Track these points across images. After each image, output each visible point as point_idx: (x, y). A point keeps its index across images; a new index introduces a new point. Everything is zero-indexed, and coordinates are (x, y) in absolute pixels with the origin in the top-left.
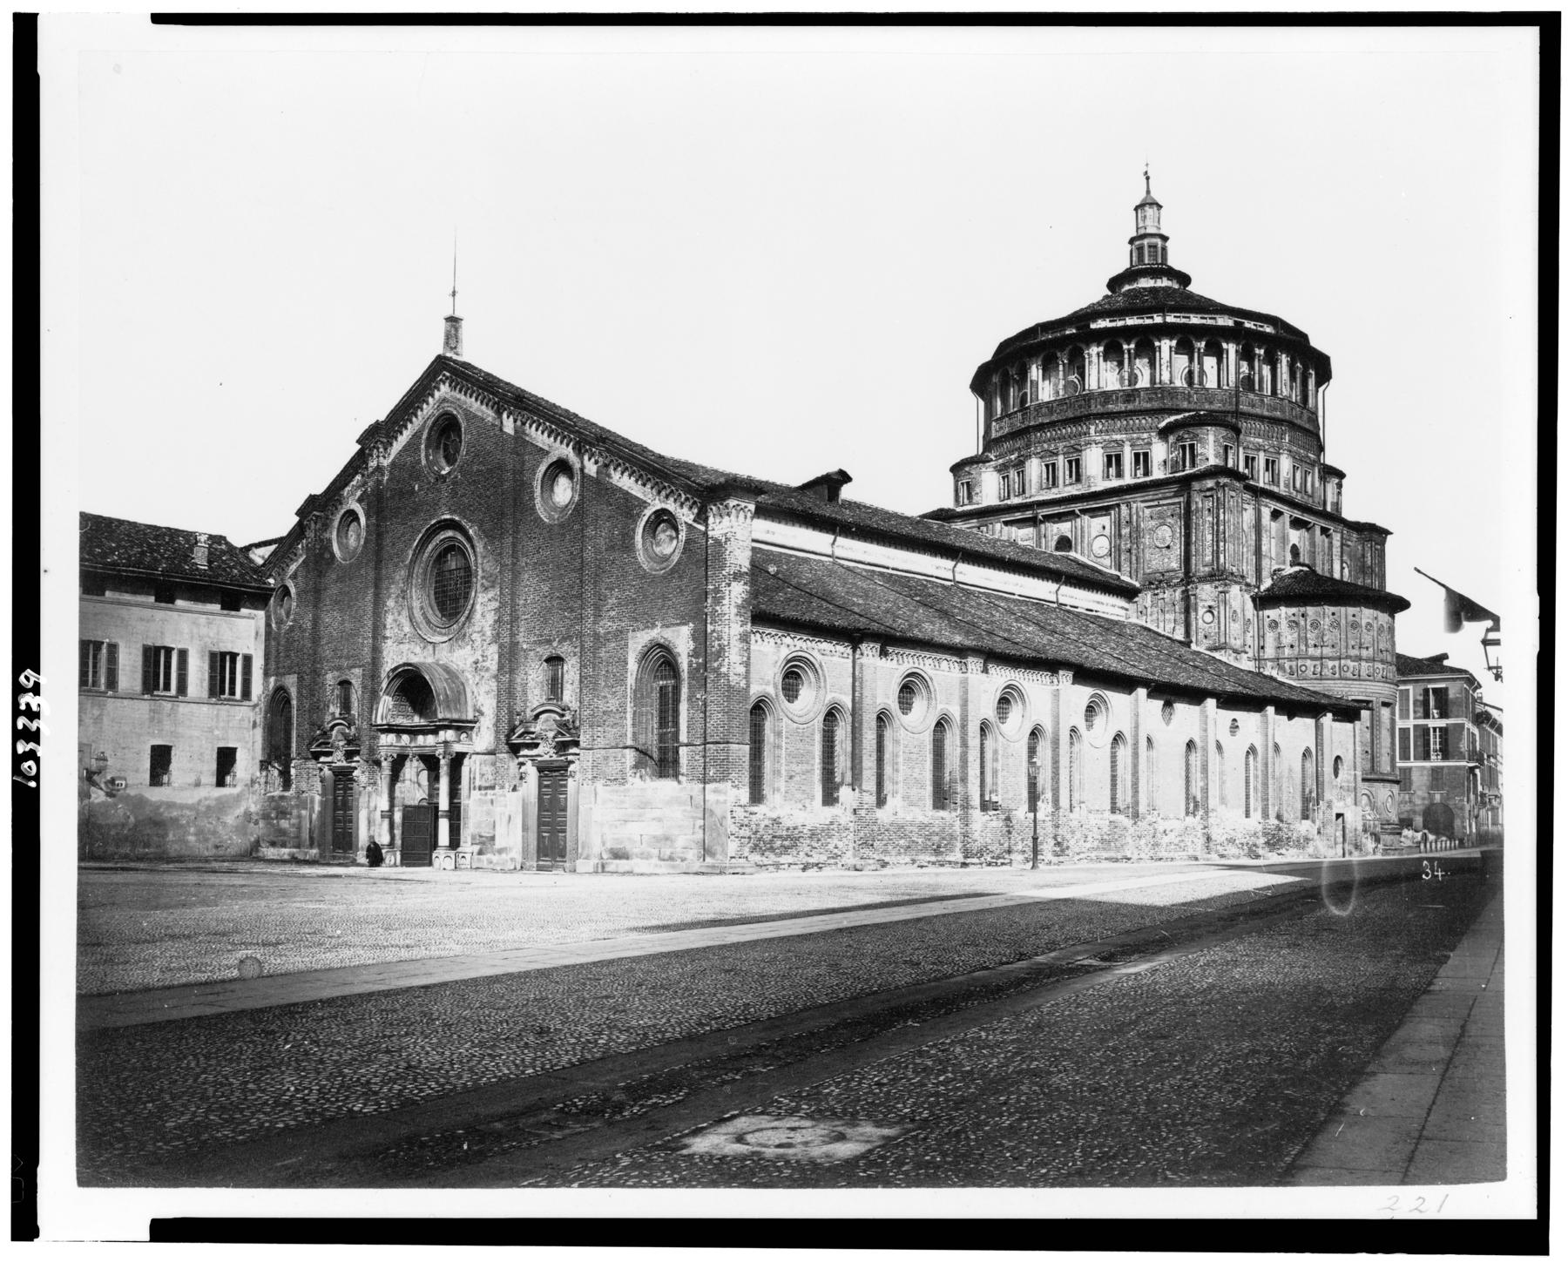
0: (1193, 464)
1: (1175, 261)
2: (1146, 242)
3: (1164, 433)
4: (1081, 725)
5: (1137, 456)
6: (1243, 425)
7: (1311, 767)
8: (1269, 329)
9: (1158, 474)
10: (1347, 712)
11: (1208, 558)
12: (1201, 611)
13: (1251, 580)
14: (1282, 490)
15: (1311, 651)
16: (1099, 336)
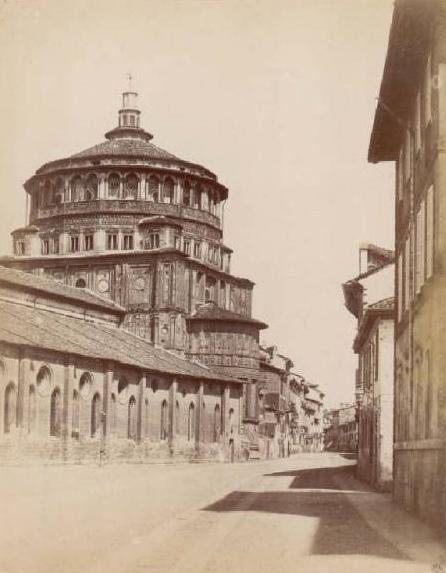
0: (158, 246)
1: (145, 125)
2: (129, 114)
3: (142, 227)
4: (116, 393)
5: (125, 238)
6: (184, 225)
7: (218, 415)
8: (197, 174)
9: (137, 249)
10: (237, 388)
11: (166, 298)
12: (161, 327)
13: (187, 311)
14: (202, 261)
15: (218, 351)
16: (105, 169)
